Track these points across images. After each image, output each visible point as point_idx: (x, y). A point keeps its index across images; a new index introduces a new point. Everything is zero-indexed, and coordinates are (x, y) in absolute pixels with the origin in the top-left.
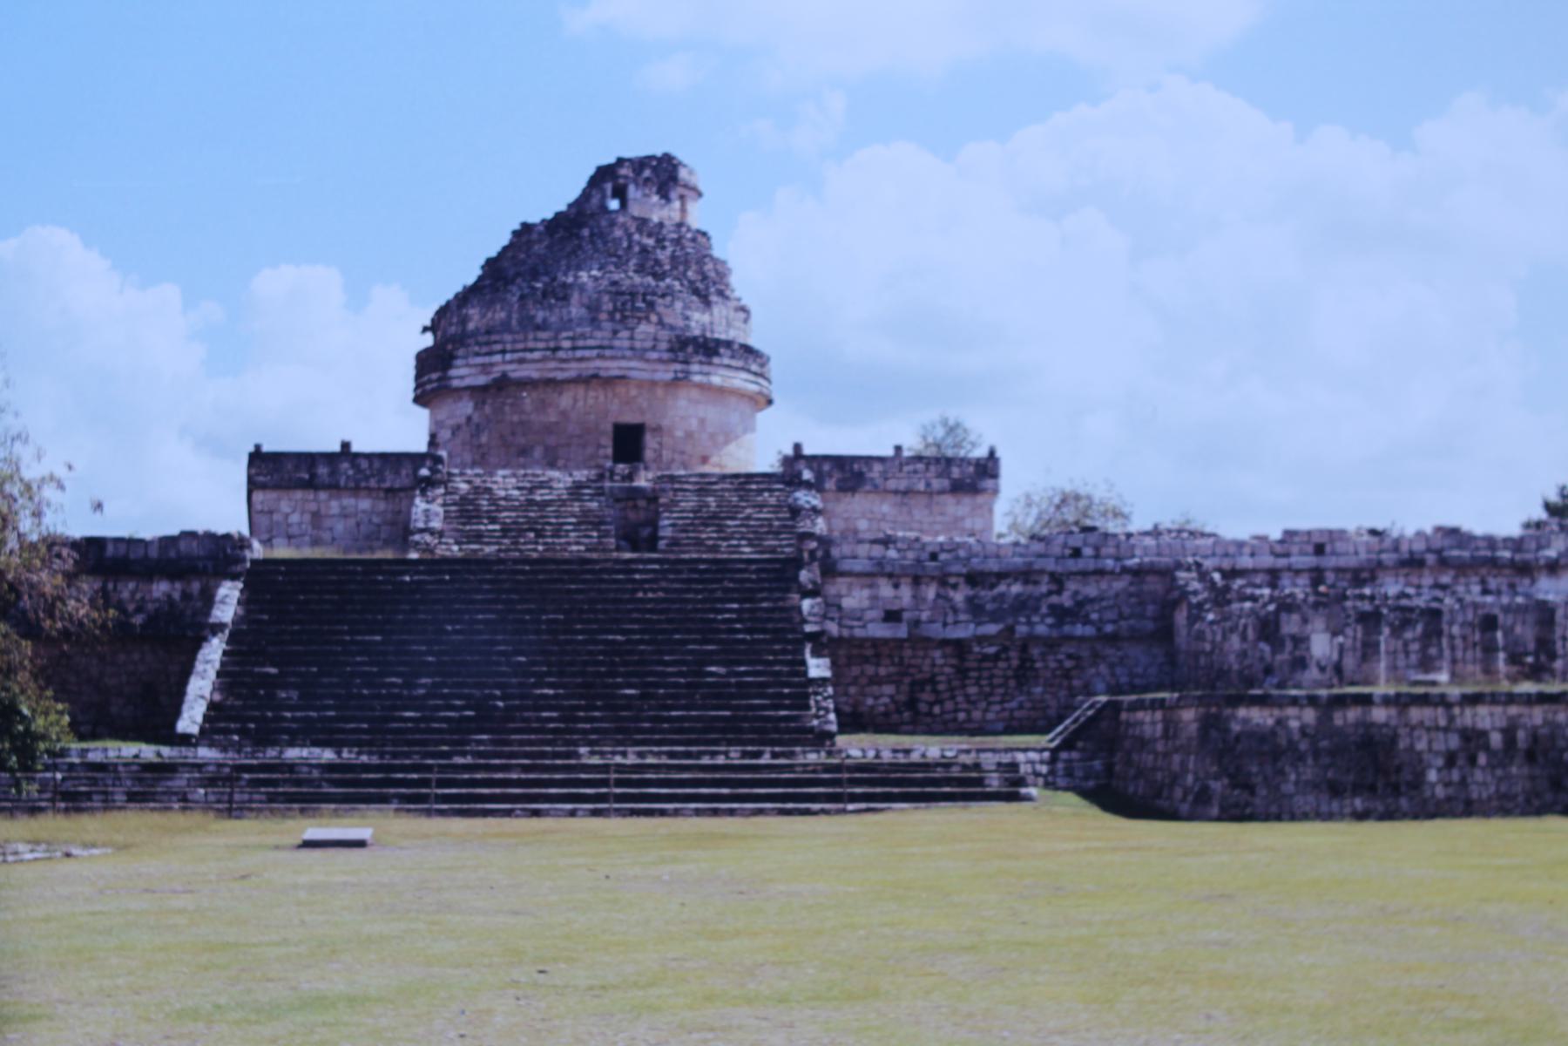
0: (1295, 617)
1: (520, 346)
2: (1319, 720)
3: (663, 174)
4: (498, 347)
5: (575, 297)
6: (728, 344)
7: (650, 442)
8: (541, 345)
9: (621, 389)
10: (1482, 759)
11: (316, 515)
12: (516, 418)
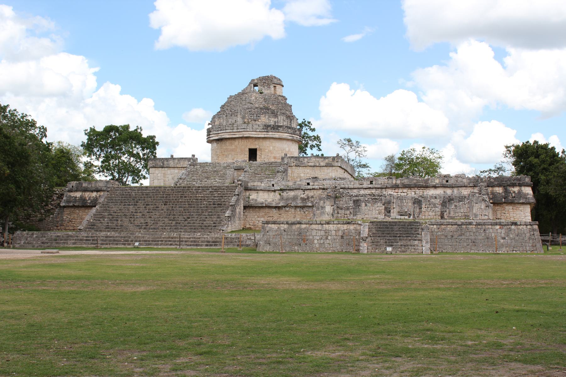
0: (322, 202)
1: (224, 129)
2: (288, 228)
3: (269, 81)
5: (239, 116)
6: (281, 126)
7: (258, 153)
8: (229, 128)
9: (251, 140)
10: (329, 238)
11: (164, 174)
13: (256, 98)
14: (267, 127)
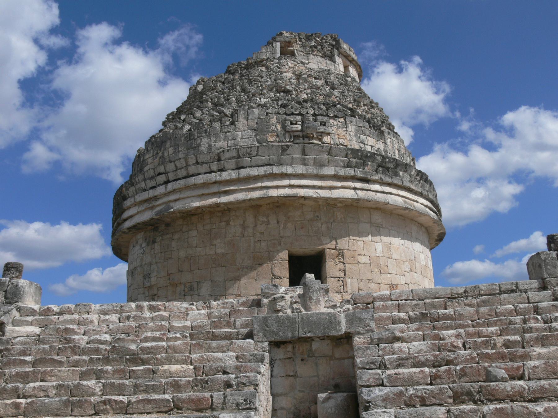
1: (183, 173)
4: (162, 178)
12: (182, 254)
13: (298, 76)
14: (361, 157)
